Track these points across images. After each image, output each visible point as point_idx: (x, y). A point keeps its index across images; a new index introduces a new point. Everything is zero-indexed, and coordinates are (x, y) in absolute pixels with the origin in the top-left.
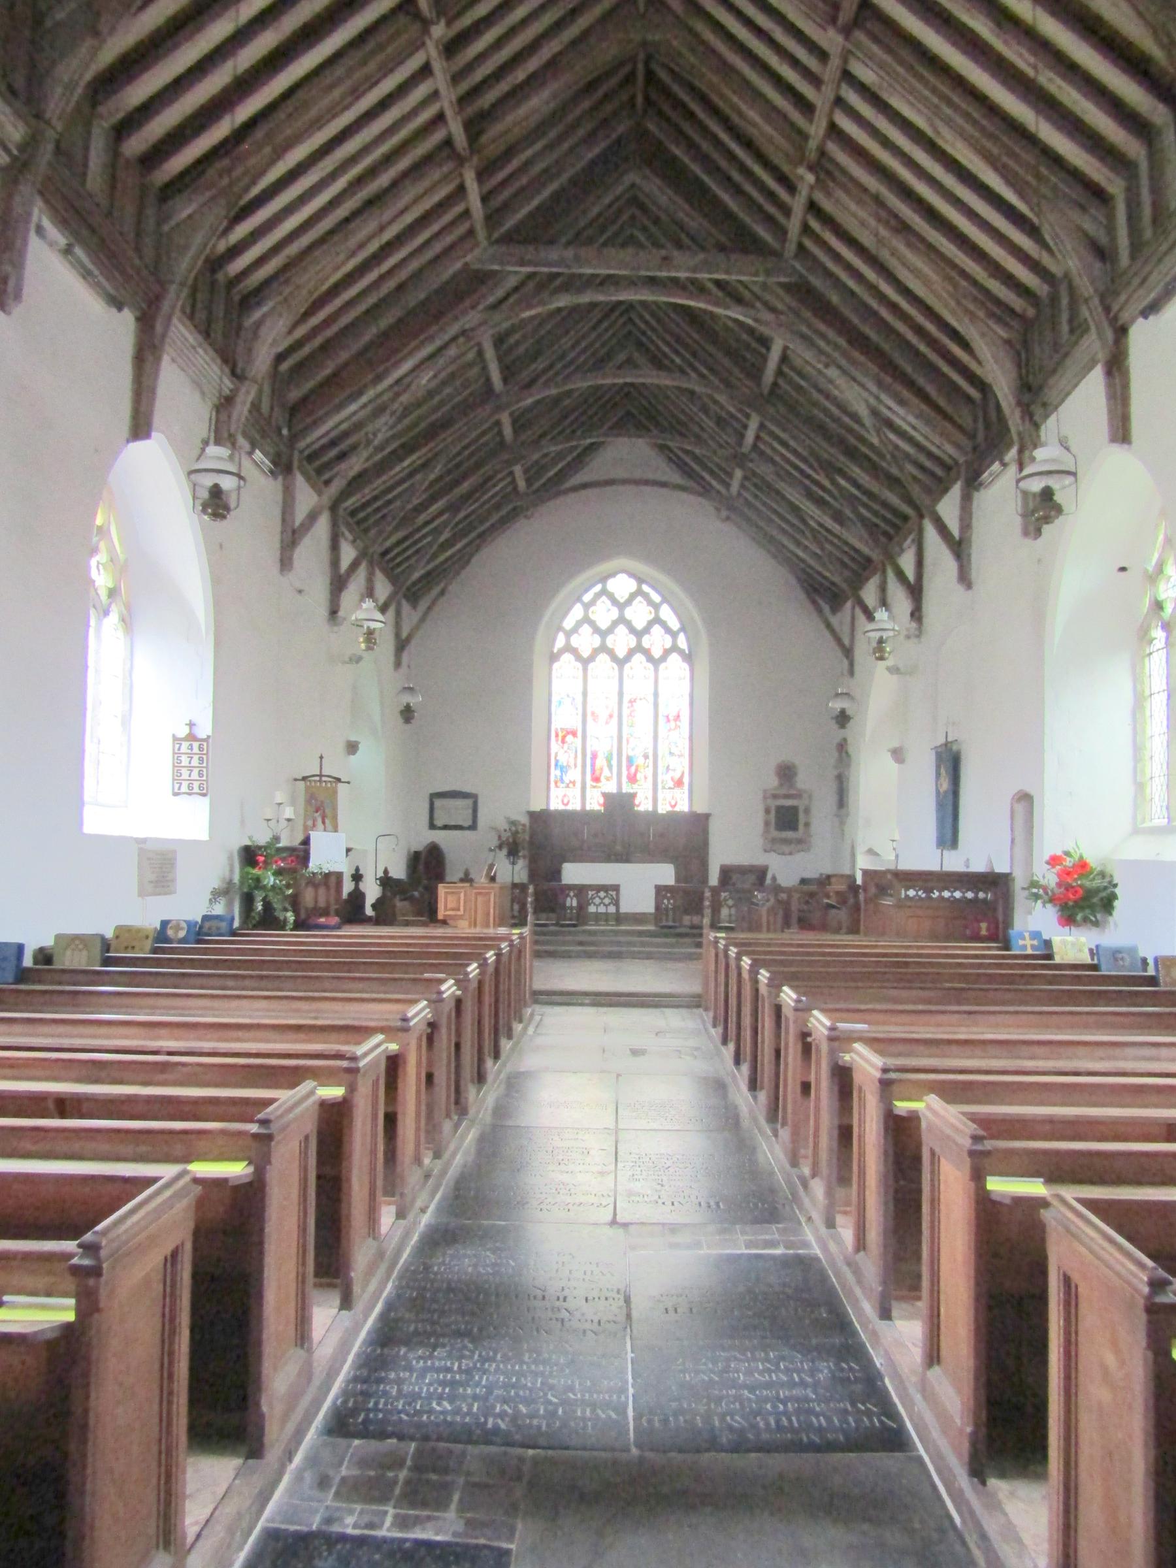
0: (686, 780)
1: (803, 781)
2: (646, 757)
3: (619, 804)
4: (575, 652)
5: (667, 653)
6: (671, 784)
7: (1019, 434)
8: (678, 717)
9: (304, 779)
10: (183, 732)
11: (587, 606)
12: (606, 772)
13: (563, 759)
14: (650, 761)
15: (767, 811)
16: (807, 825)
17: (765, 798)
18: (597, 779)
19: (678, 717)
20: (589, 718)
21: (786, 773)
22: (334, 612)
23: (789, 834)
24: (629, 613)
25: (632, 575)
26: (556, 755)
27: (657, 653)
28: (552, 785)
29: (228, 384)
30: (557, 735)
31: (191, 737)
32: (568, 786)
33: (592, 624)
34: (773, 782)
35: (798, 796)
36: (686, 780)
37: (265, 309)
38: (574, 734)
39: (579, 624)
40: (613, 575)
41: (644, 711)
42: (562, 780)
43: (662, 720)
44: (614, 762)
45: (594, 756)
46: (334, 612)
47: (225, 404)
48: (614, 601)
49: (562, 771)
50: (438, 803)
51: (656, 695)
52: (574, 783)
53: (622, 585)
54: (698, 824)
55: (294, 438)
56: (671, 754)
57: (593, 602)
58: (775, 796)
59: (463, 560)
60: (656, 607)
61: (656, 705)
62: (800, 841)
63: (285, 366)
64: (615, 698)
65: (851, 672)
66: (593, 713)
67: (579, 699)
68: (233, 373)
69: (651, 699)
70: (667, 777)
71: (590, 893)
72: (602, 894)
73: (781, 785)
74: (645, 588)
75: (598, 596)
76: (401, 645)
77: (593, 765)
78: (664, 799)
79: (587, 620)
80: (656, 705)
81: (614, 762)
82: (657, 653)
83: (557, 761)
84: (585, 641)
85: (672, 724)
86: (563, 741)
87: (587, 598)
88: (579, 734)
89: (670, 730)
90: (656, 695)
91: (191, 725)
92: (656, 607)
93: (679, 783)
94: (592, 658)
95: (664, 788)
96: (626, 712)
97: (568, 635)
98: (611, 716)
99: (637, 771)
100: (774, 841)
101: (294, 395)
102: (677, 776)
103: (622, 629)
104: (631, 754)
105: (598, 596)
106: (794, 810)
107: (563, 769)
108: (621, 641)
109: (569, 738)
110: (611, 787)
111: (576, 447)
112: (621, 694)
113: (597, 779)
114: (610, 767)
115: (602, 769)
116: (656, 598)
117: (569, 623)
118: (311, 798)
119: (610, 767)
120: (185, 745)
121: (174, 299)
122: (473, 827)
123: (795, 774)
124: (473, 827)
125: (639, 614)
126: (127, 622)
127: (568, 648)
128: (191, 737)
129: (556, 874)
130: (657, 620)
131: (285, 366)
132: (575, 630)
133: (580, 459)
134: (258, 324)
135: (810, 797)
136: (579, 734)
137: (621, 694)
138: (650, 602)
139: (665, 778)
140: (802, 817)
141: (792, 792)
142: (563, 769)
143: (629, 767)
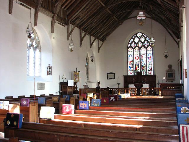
0: (152, 69)
1: (173, 68)
2: (145, 65)
3: (139, 74)
4: (132, 47)
5: (148, 46)
7: (178, 4)
8: (150, 58)
9: (74, 72)
10: (48, 66)
11: (133, 39)
12: (138, 68)
13: (130, 66)
14: (146, 66)
15: (167, 74)
16: (174, 76)
17: (166, 72)
18: (136, 69)
19: (150, 58)
20: (135, 59)
21: (170, 67)
22: (81, 45)
23: (171, 78)
24: (141, 39)
25: (141, 33)
27: (146, 46)
29: (53, 15)
31: (49, 67)
33: (135, 42)
34: (167, 68)
35: (172, 71)
36: (152, 69)
37: (58, 3)
39: (132, 42)
40: (138, 33)
41: (144, 57)
43: (147, 58)
44: (139, 66)
45: (136, 65)
46: (81, 45)
47: (53, 18)
48: (138, 38)
50: (108, 75)
51: (146, 54)
52: (132, 70)
53: (139, 35)
54: (154, 76)
55: (68, 20)
56: (150, 64)
57: (134, 38)
58: (168, 71)
59: (109, 34)
60: (146, 38)
61: (146, 55)
62: (173, 79)
63: (65, 9)
64: (139, 55)
65: (179, 47)
66: (135, 58)
67: (133, 55)
68: (53, 13)
69: (145, 54)
70: (149, 69)
71: (147, 90)
72: (132, 90)
73: (169, 69)
74: (144, 35)
75: (135, 37)
76: (99, 48)
77: (135, 67)
79: (133, 41)
80: (146, 55)
81: (139, 66)
82: (146, 46)
84: (133, 45)
85: (150, 59)
86: (130, 63)
87: (133, 38)
90: (146, 54)
91: (49, 65)
92: (146, 38)
93: (151, 69)
94: (148, 47)
96: (141, 57)
97: (130, 44)
98: (138, 58)
100: (168, 79)
101: (68, 13)
102: (151, 68)
103: (140, 43)
105: (135, 37)
106: (172, 73)
107: (131, 68)
108: (140, 44)
109: (131, 62)
110: (139, 71)
111: (126, 12)
112: (140, 54)
113: (136, 69)
114: (139, 67)
116: (146, 36)
117: (130, 42)
118: (75, 75)
119: (139, 67)
120: (49, 68)
121: (39, 6)
122: (114, 79)
123: (172, 67)
124: (114, 79)
125: (143, 40)
126: (40, 51)
127: (131, 47)
128: (49, 67)
129: (128, 87)
130: (146, 40)
131: (65, 9)
132: (132, 43)
133: (130, 13)
134: (57, 5)
135: (175, 71)
137: (140, 54)
138: (144, 37)
139: (149, 69)
140: (173, 75)
141: (171, 70)
142: (131, 68)
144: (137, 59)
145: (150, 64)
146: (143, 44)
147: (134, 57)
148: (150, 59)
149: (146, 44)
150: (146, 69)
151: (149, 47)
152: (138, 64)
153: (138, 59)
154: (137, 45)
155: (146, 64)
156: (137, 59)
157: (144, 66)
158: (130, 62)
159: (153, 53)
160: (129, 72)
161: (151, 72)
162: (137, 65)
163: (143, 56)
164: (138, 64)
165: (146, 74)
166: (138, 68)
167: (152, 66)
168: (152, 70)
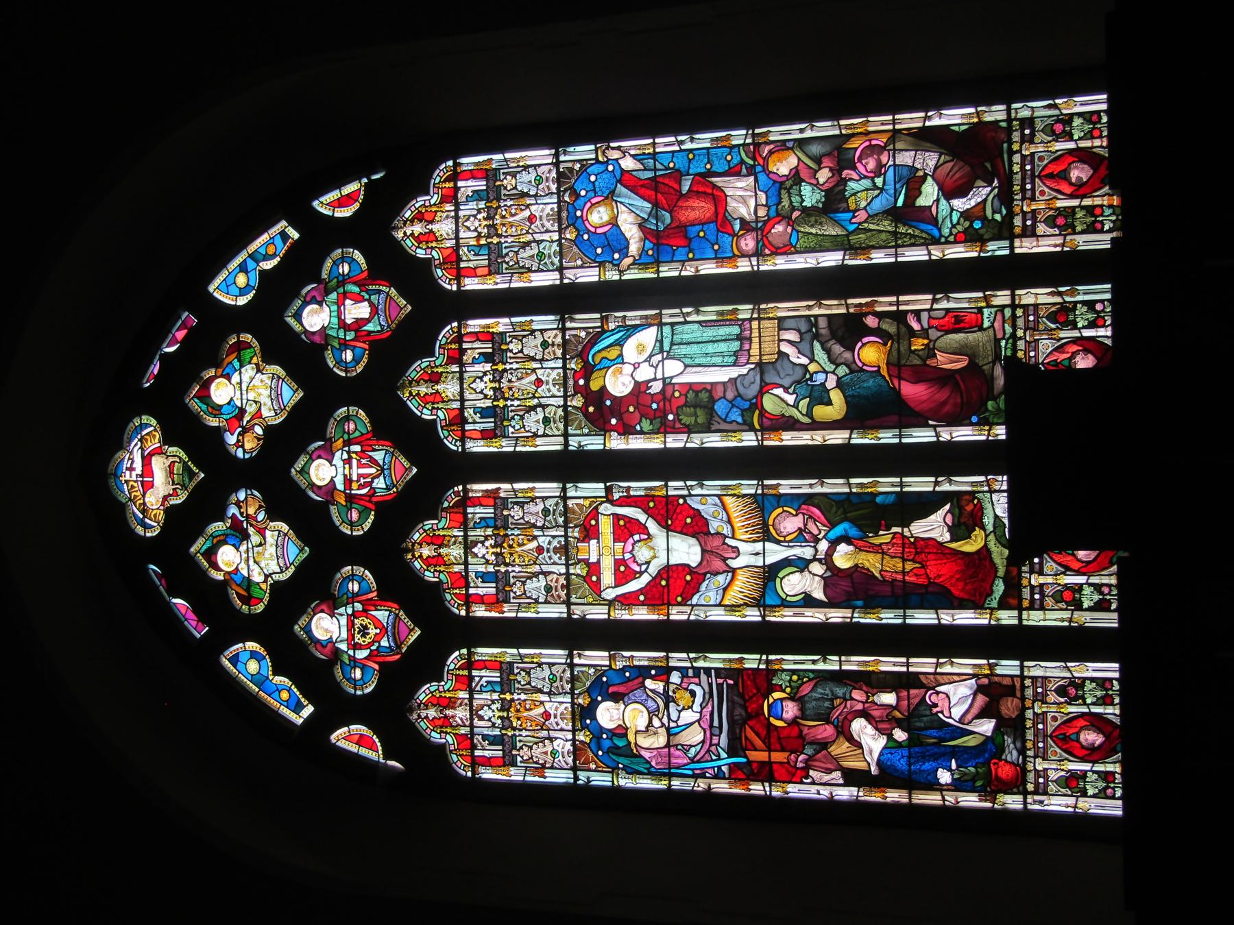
0: (954, 117)
6: (981, 193)
12: (934, 527)
26: (853, 777)
28: (1012, 802)
30: (766, 773)
32: (1013, 726)
36: (954, 117)
38: (764, 681)
42: (991, 748)
49: (943, 756)
56: (835, 200)
66: (656, 595)
67: (597, 657)
69: (584, 322)
78: (1064, 221)
81: (886, 485)
83: (886, 777)
86: (792, 739)
88: (752, 661)
89: (721, 220)
95: (1005, 231)
99: (924, 373)
102: (928, 160)
104: (836, 407)
115: (926, 546)
136: (752, 661)
143: (909, 417)
144: (686, 551)
145: (835, 200)
146: (351, 391)
147: (641, 614)
148: (699, 209)
149: (357, 311)
150: (961, 300)
151: (407, 232)
152: (835, 509)
153: (697, 527)
154: (356, 551)
155: (834, 307)
156: (686, 551)
157: (871, 354)
158: (772, 738)
159: (558, 137)
160: (1058, 803)
161: (1045, 148)
162: (843, 557)
163: (618, 384)
164: (835, 509)
165: (1101, 292)
166: (934, 527)
167: (879, 122)
168: (996, 113)
